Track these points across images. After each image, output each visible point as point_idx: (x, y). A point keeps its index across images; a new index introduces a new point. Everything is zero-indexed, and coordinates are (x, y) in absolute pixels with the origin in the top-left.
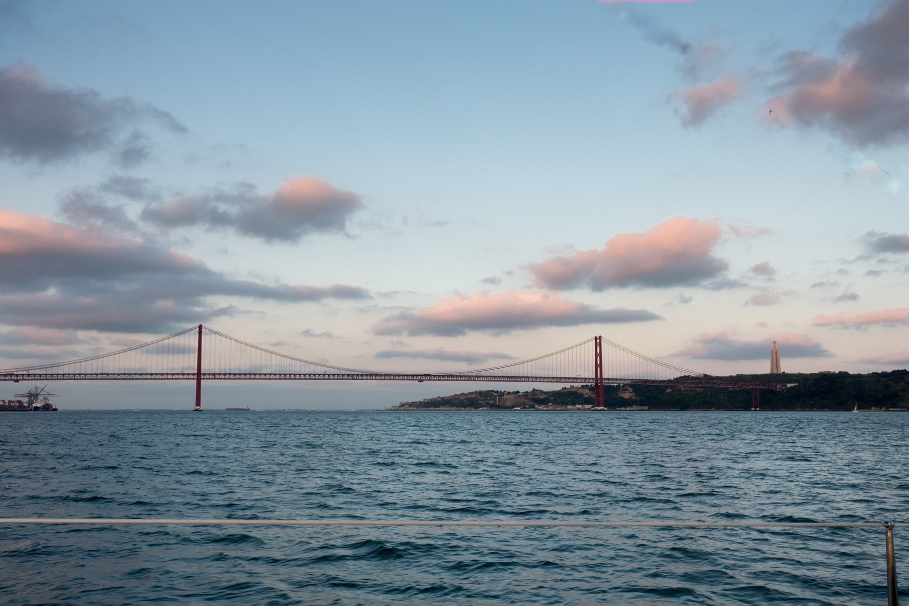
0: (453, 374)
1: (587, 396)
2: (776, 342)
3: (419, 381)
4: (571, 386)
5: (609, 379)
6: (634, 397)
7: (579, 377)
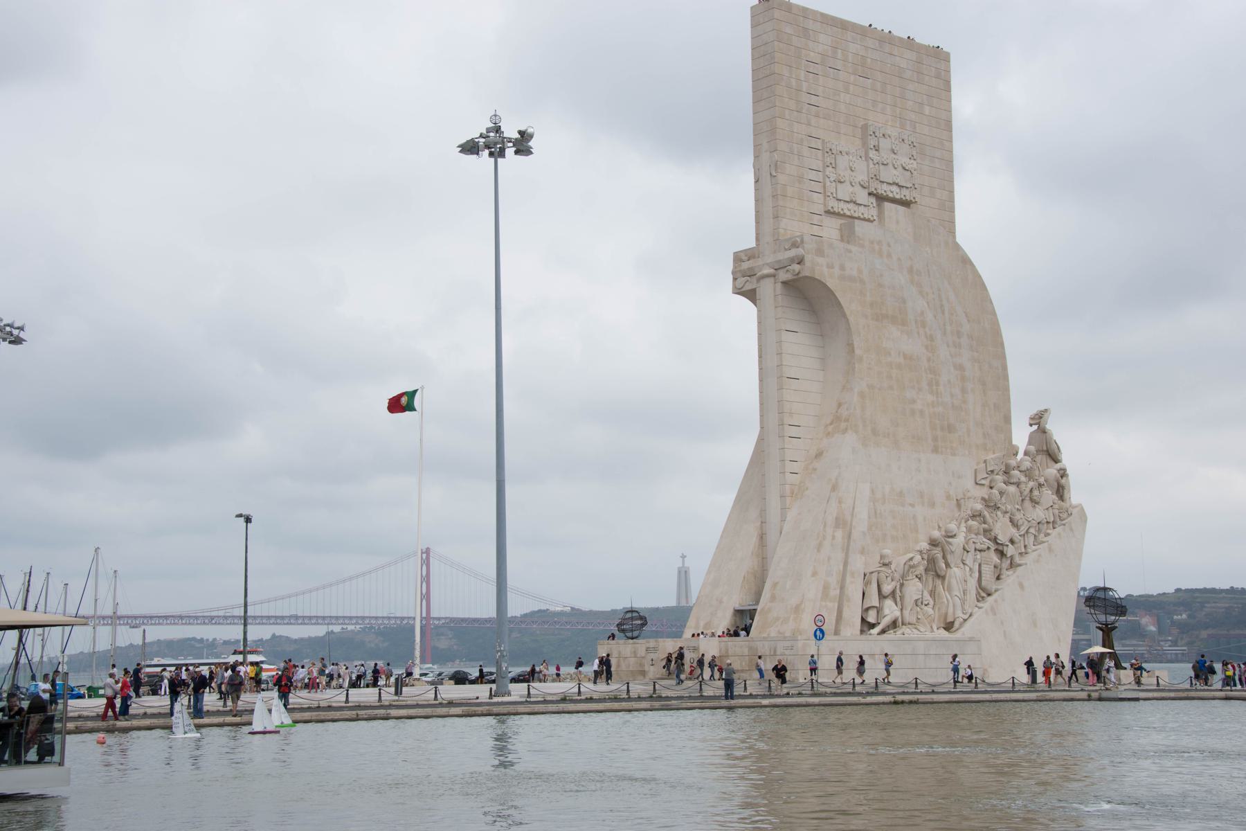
0: (184, 614)
1: (373, 645)
2: (685, 556)
3: (131, 627)
4: (343, 629)
5: (439, 619)
6: (455, 647)
7: (392, 615)
